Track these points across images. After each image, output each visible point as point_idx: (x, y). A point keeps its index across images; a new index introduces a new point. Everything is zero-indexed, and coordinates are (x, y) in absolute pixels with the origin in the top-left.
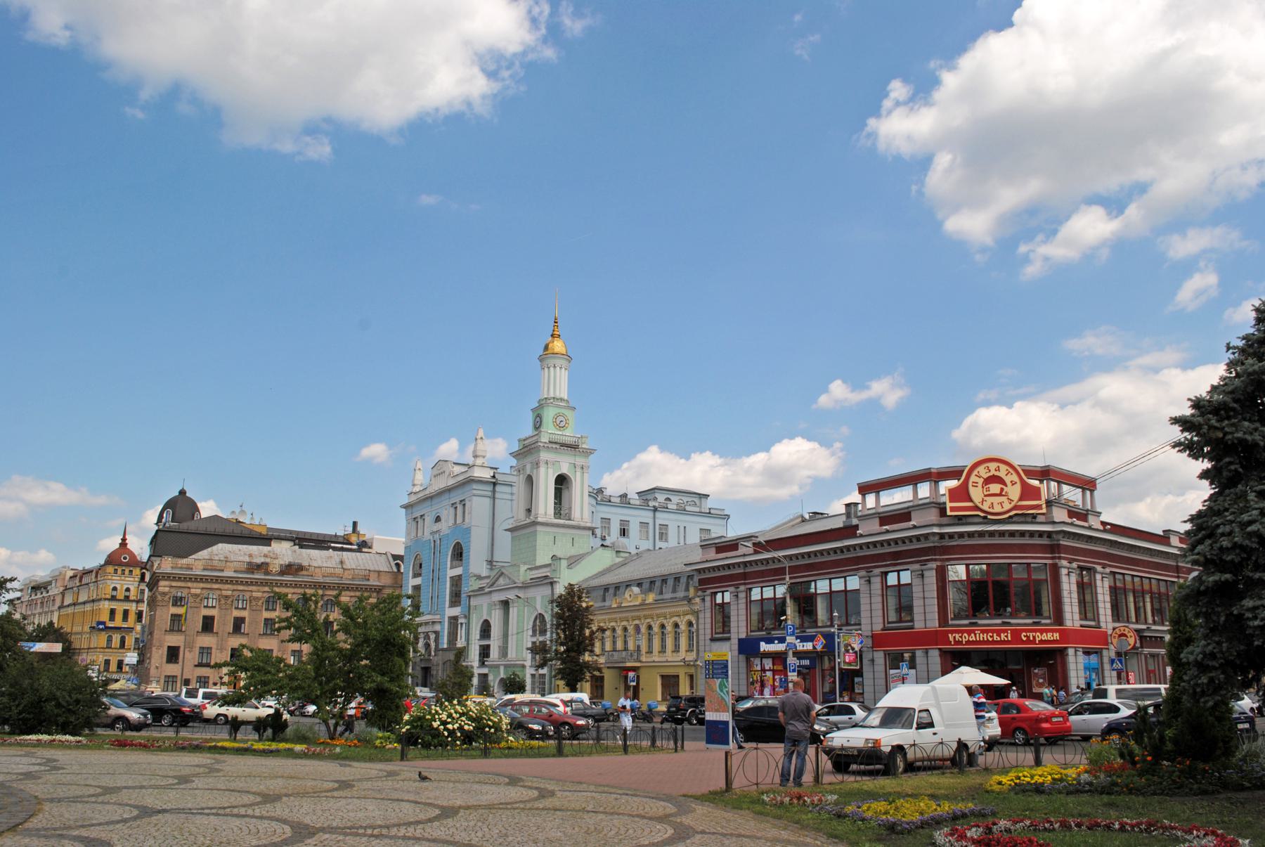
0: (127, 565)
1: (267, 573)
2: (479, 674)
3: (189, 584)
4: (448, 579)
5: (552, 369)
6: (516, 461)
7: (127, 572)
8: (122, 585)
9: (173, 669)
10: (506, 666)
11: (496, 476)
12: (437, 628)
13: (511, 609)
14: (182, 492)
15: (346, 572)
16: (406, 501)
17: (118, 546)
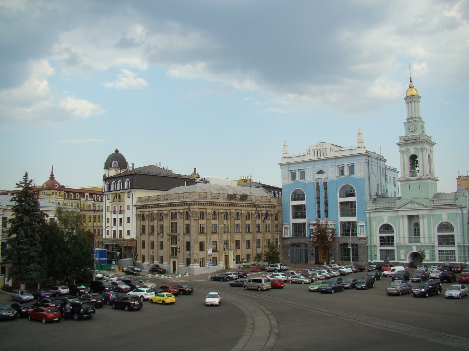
0: (58, 189)
1: (235, 199)
2: (381, 250)
3: (206, 207)
4: (339, 203)
5: (413, 103)
6: (399, 147)
7: (58, 194)
8: (56, 201)
9: (202, 254)
10: (418, 247)
11: (368, 152)
12: (332, 227)
13: (420, 219)
14: (117, 151)
15: (263, 198)
16: (281, 162)
17: (49, 179)
